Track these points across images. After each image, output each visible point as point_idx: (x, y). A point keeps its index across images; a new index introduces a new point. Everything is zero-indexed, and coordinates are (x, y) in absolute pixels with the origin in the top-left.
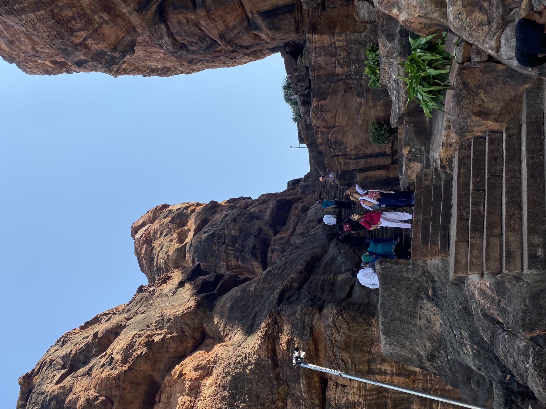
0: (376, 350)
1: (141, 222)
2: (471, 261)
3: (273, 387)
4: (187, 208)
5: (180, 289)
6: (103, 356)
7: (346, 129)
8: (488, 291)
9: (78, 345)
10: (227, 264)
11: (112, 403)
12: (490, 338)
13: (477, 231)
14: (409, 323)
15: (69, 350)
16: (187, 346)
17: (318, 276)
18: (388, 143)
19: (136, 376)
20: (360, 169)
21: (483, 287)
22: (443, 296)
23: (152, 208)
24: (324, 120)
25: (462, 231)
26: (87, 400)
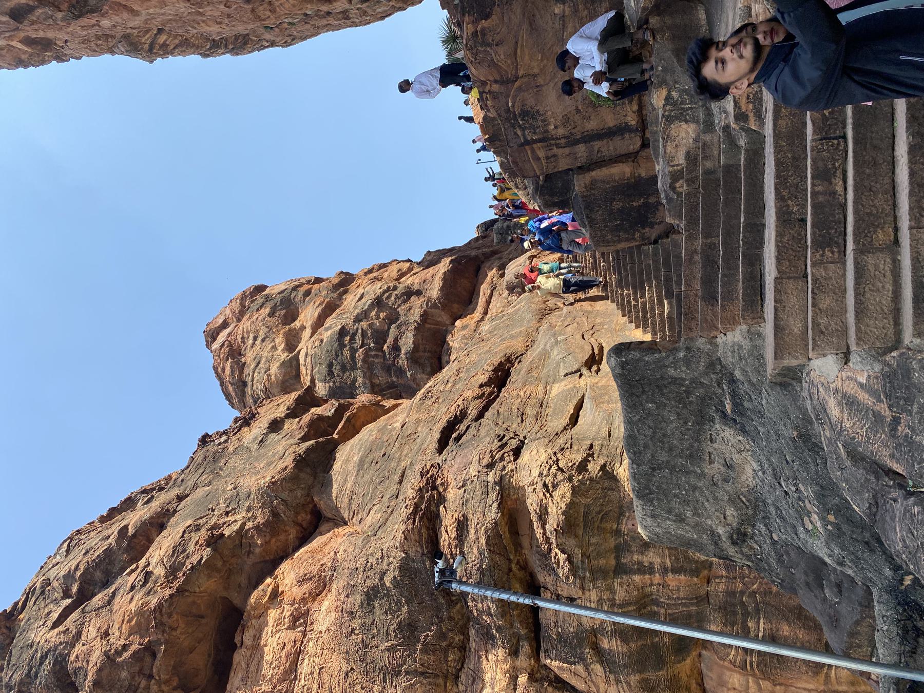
0: (630, 526)
1: (221, 321)
2: (816, 324)
3: (438, 609)
4: (295, 288)
5: (272, 435)
6: (133, 571)
7: (540, 81)
8: (864, 397)
9: (92, 552)
11: (154, 655)
12: (869, 508)
13: (829, 245)
14: (688, 473)
15: (73, 564)
16: (287, 540)
17: (512, 392)
18: (630, 102)
19: (194, 603)
20: (579, 168)
21: (851, 389)
22: (755, 413)
23: (237, 293)
24: (493, 64)
26: (106, 654)
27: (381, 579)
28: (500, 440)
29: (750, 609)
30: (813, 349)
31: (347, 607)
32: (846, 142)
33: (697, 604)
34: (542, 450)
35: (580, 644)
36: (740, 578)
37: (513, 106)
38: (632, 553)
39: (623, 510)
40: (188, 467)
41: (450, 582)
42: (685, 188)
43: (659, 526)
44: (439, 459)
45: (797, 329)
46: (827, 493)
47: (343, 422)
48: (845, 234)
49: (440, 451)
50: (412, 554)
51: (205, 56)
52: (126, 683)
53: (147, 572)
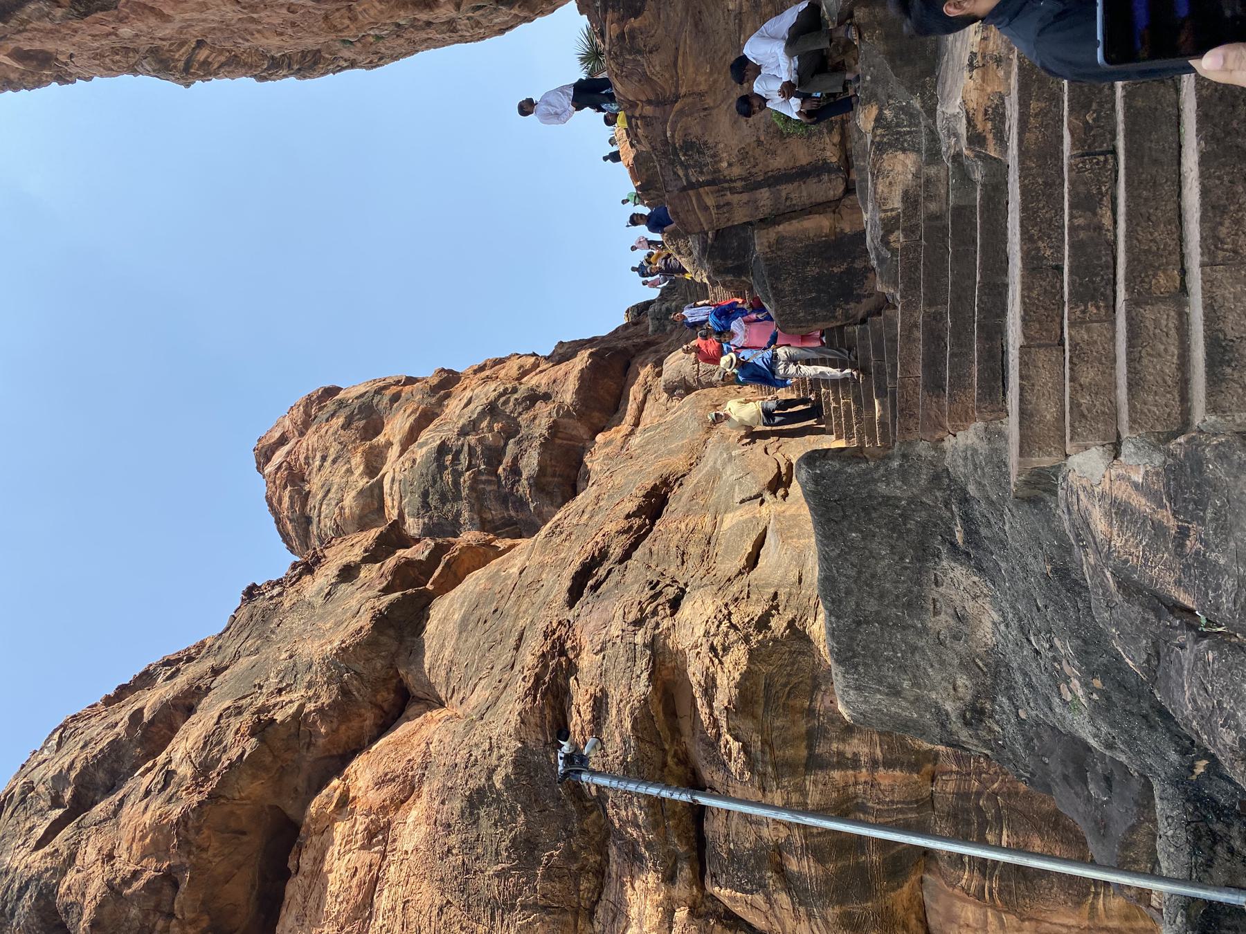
0: (827, 703)
1: (277, 435)
2: (1075, 405)
3: (567, 819)
4: (379, 391)
5: (343, 586)
6: (149, 770)
7: (709, 101)
8: (1141, 503)
9: (92, 745)
10: (481, 517)
11: (176, 886)
12: (1148, 661)
13: (1093, 298)
14: (904, 628)
15: (67, 761)
16: (362, 728)
17: (670, 524)
18: (830, 132)
19: (232, 813)
20: (761, 220)
23: (300, 396)
24: (646, 79)
25: (1040, 313)
26: (109, 884)
27: (489, 778)
28: (652, 588)
29: (989, 816)
30: (1071, 439)
31: (442, 817)
32: (1116, 159)
33: (918, 810)
34: (709, 601)
35: (759, 866)
36: (975, 774)
37: (673, 136)
38: (830, 740)
39: (818, 681)
40: (228, 629)
41: (579, 772)
42: (901, 240)
43: (866, 702)
44: (569, 615)
45: (1049, 414)
46: (1092, 648)
47: (440, 568)
48: (1115, 283)
49: (571, 603)
50: (531, 743)
51: (262, 79)
52: (137, 923)
53: (168, 772)
